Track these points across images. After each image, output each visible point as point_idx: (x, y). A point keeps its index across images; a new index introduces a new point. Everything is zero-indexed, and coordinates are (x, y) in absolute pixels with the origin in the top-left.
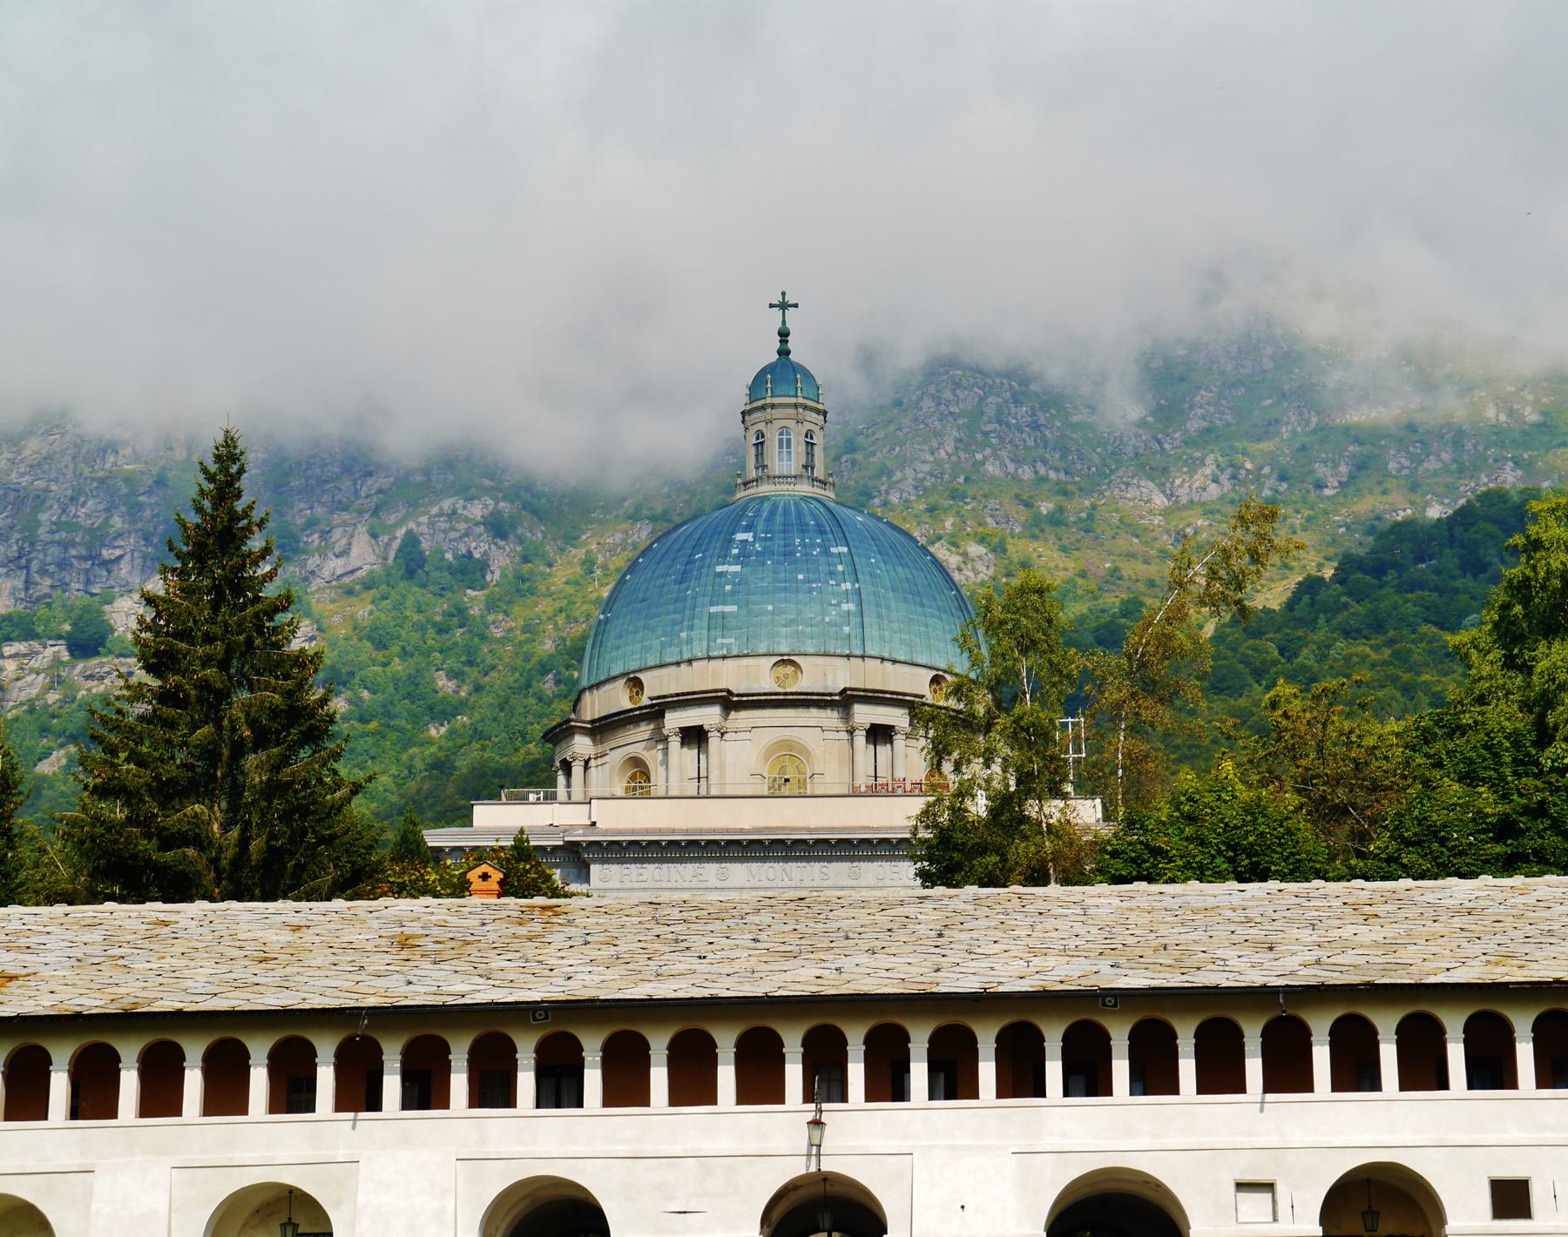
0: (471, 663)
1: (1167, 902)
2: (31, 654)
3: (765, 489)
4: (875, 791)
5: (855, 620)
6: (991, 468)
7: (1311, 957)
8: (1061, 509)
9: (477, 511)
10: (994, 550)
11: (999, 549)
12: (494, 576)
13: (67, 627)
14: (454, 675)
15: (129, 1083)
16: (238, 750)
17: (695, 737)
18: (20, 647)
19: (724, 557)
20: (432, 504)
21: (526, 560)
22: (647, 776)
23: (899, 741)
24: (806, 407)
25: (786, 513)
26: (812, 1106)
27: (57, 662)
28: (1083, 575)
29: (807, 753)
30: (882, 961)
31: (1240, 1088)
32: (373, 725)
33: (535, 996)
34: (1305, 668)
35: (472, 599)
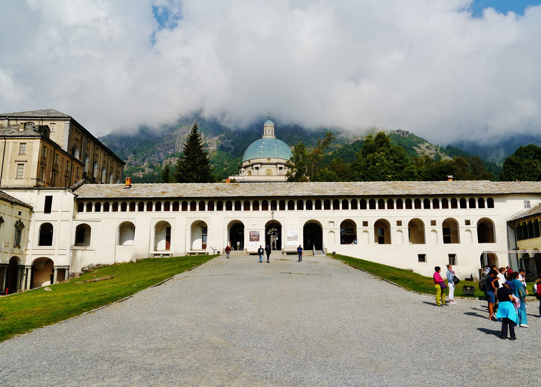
0: (229, 161)
1: (320, 184)
2: (175, 159)
3: (266, 137)
4: (280, 175)
5: (278, 154)
7: (340, 192)
8: (304, 142)
9: (230, 141)
12: (232, 150)
13: (179, 156)
14: (227, 162)
15: (180, 207)
16: (197, 165)
17: (257, 168)
18: (173, 158)
19: (261, 145)
20: (225, 140)
21: (236, 148)
22: (251, 173)
23: (283, 169)
24: (272, 126)
25: (269, 140)
26: (272, 211)
29: (271, 170)
30: (282, 192)
31: (330, 209)
32: (217, 168)
33: (235, 196)
35: (229, 153)
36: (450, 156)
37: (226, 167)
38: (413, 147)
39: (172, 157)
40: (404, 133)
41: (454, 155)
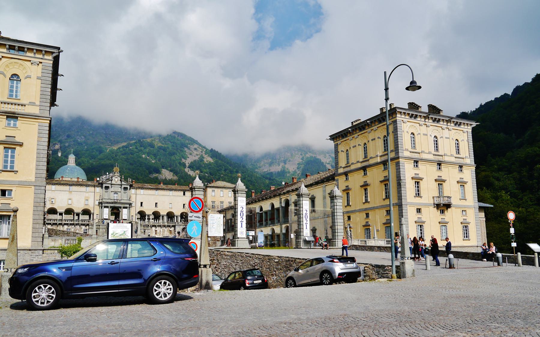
3: (70, 164)
6: (85, 127)
10: (84, 137)
11: (85, 137)
19: (67, 170)
28: (95, 141)
34: (117, 158)
36: (211, 157)
38: (185, 148)
41: (214, 157)
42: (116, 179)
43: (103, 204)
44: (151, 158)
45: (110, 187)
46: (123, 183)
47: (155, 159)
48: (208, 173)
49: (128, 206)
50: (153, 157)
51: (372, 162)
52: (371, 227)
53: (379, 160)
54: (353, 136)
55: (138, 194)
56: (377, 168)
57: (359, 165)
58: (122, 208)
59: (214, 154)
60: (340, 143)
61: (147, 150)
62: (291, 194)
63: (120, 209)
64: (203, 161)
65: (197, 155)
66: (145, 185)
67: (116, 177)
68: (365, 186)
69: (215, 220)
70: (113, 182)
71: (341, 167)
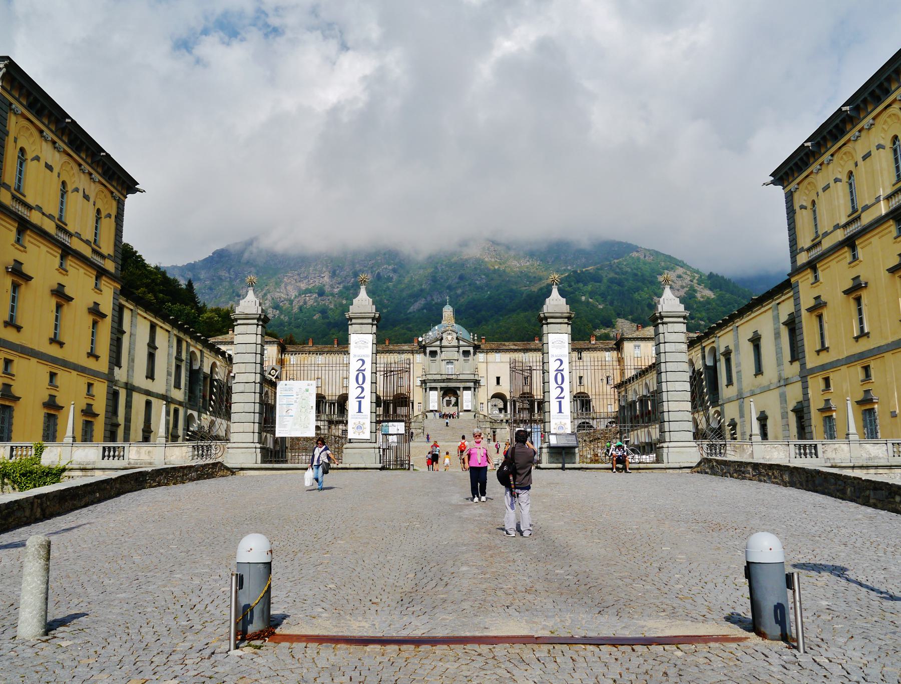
2: (311, 296)
9: (390, 267)
14: (387, 300)
18: (309, 295)
21: (400, 277)
27: (316, 297)
36: (711, 289)
37: (387, 308)
38: (658, 276)
39: (307, 293)
40: (648, 254)
41: (717, 288)
42: (450, 337)
43: (428, 384)
44: (597, 301)
45: (439, 352)
46: (461, 343)
47: (604, 301)
48: (706, 319)
49: (472, 385)
50: (600, 299)
51: (867, 218)
52: (876, 406)
53: (883, 209)
54: (820, 161)
55: (492, 362)
56: (881, 234)
57: (840, 235)
58: (461, 389)
59: (714, 281)
60: (796, 186)
61: (589, 288)
62: (718, 335)
63: (458, 392)
64: (695, 297)
65: (683, 287)
66: (504, 345)
67: (448, 332)
68: (856, 289)
69: (295, 396)
70: (444, 343)
71: (802, 250)
